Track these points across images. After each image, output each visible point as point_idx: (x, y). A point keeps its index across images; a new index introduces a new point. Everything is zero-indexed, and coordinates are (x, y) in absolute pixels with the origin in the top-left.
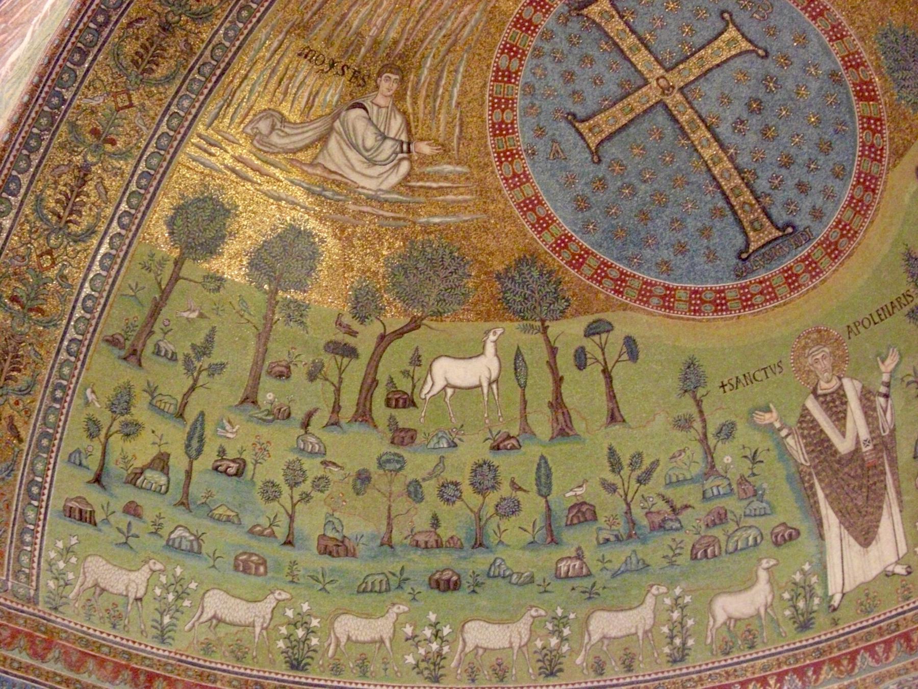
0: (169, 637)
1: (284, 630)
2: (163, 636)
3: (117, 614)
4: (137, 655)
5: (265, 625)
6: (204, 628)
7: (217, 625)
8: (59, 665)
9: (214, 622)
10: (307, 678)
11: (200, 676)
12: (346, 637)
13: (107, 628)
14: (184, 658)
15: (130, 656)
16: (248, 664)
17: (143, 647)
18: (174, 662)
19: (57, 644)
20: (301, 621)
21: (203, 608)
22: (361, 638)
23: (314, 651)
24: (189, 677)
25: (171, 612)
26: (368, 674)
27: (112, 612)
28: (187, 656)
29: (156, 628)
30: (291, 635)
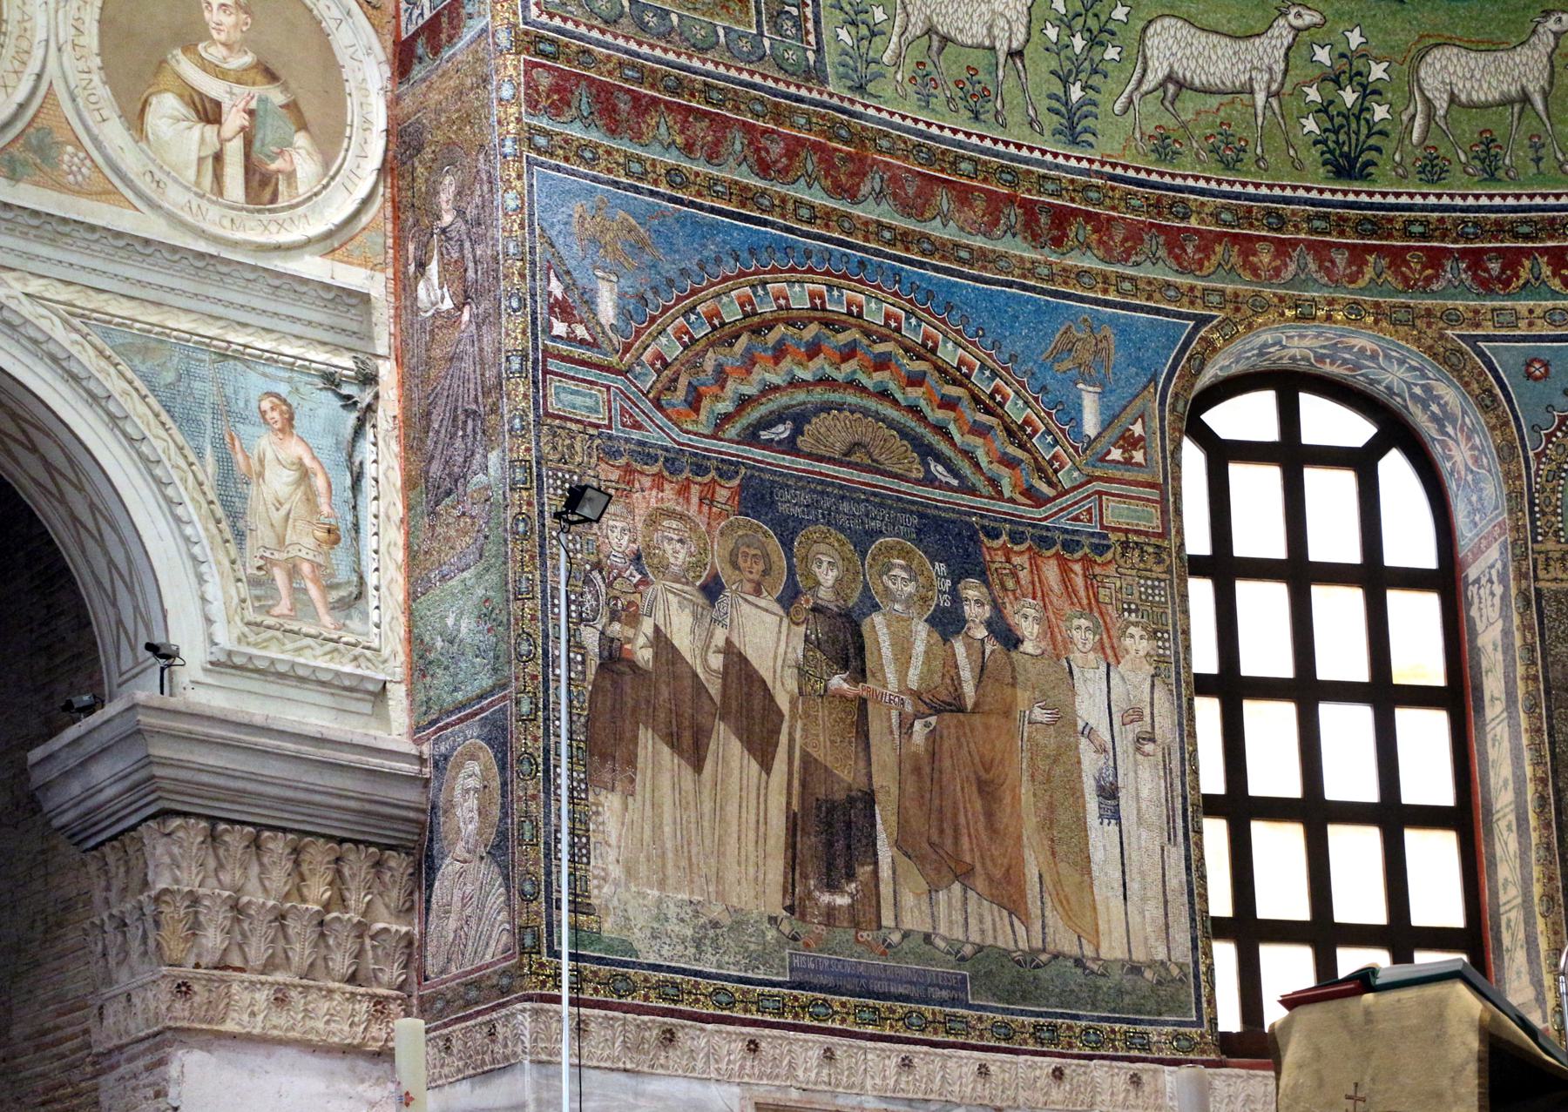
0: (1086, 130)
1: (1313, 94)
2: (1072, 127)
5: (1274, 87)
6: (1152, 104)
7: (1176, 96)
8: (885, 206)
9: (1171, 88)
10: (1371, 194)
11: (1156, 206)
12: (1445, 96)
13: (963, 121)
14: (1119, 171)
15: (1015, 178)
16: (1248, 173)
17: (1037, 154)
18: (1100, 182)
20: (1347, 71)
21: (1145, 57)
22: (1479, 96)
23: (1382, 133)
24: (1134, 210)
25: (1083, 76)
26: (1501, 174)
28: (1126, 168)
29: (1058, 113)
30: (1331, 102)
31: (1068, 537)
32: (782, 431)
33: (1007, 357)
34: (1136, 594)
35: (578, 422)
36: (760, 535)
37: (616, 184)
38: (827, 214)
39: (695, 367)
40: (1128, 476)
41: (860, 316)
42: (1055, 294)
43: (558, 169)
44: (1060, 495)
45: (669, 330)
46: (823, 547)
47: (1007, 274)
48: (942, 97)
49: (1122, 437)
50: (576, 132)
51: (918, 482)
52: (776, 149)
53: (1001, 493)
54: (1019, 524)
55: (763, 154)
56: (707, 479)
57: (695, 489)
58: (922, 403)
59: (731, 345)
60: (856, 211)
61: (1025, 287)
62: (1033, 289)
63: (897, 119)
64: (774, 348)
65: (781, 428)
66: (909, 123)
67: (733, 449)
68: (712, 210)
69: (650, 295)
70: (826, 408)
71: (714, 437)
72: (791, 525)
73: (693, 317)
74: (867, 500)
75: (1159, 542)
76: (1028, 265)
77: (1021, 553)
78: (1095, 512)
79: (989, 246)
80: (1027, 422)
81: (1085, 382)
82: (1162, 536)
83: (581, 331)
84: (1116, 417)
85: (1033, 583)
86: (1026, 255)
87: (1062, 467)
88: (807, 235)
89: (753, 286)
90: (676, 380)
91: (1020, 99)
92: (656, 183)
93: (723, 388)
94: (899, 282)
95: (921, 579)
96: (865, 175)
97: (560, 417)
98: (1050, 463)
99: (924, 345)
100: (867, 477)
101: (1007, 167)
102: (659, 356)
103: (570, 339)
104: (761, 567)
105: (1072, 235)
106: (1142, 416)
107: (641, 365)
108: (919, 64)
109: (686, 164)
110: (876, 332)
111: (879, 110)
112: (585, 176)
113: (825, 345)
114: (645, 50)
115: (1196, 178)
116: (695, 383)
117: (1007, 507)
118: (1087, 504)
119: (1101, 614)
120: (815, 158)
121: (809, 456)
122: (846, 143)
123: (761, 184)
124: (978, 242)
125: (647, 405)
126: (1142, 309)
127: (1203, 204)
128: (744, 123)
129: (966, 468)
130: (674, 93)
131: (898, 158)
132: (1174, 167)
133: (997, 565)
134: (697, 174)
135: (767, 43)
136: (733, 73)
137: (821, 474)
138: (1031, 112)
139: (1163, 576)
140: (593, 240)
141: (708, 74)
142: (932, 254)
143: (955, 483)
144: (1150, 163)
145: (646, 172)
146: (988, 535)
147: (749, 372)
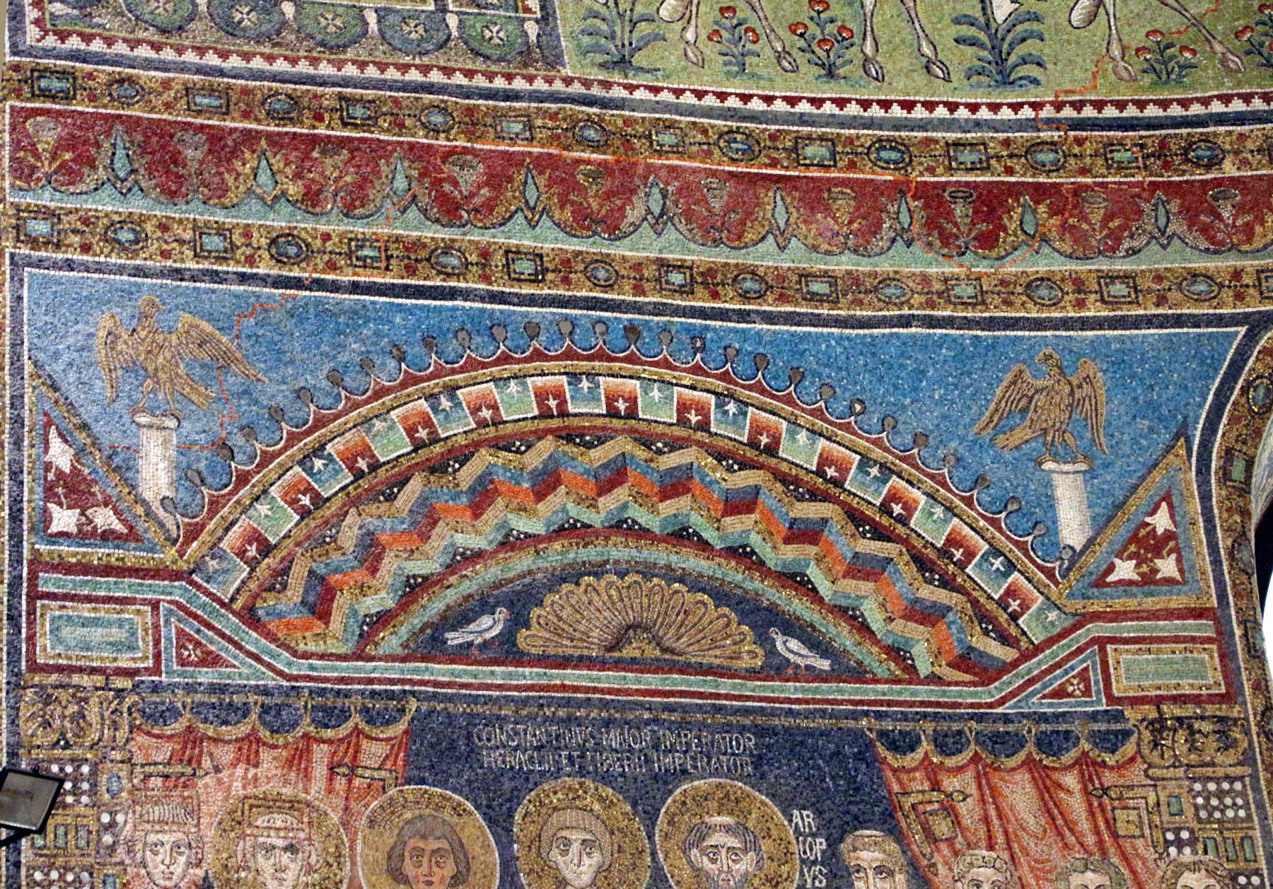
2: (1001, 60)
3: (831, 29)
4: (928, 141)
8: (671, 234)
13: (808, 82)
14: (1089, 112)
17: (941, 112)
18: (1056, 135)
19: (650, 168)
24: (1121, 167)
27: (813, 29)
28: (1099, 105)
29: (973, 42)
31: (1043, 727)
32: (489, 626)
33: (908, 439)
34: (1190, 812)
35: (94, 671)
36: (447, 814)
37: (178, 274)
38: (566, 262)
39: (321, 542)
40: (1150, 603)
41: (632, 414)
42: (991, 324)
43: (70, 265)
44: (1025, 657)
45: (274, 491)
46: (569, 816)
47: (900, 306)
48: (768, 52)
49: (1134, 538)
50: (106, 204)
51: (753, 674)
52: (469, 178)
53: (912, 669)
54: (950, 717)
55: (447, 187)
56: (343, 731)
57: (321, 754)
58: (755, 540)
59: (391, 498)
60: (621, 250)
61: (932, 322)
62: (949, 322)
63: (689, 99)
64: (472, 490)
65: (486, 621)
66: (710, 101)
67: (395, 670)
68: (355, 288)
69: (238, 440)
70: (572, 574)
71: (359, 656)
72: (507, 786)
73: (318, 464)
74: (655, 721)
75: (1224, 710)
76: (937, 286)
77: (960, 769)
78: (1095, 676)
79: (864, 266)
80: (954, 541)
81: (1056, 458)
82: (1228, 698)
83: (104, 518)
84: (1120, 506)
85: (986, 820)
86: (933, 270)
87: (1025, 607)
88: (532, 301)
89: (431, 397)
90: (285, 572)
91: (907, 34)
92: (250, 261)
93: (374, 571)
94: (703, 349)
95: (766, 845)
96: (633, 191)
97: (59, 669)
98: (1002, 604)
99: (753, 444)
100: (653, 681)
101: (889, 140)
102: (256, 537)
103: (86, 534)
104: (449, 869)
105: (1012, 227)
106: (1167, 498)
107: (222, 557)
108: (722, 10)
109: (306, 225)
110: (661, 436)
111: (656, 90)
112: (120, 270)
113: (567, 472)
114: (234, 62)
115: (1226, 99)
116: (321, 570)
117: (924, 692)
118: (1078, 664)
119: (1125, 858)
120: (542, 181)
121: (544, 661)
122: (596, 147)
123: (444, 234)
124: (844, 264)
125: (230, 623)
126: (1149, 322)
127: (1242, 137)
128: (412, 146)
129: (844, 637)
130: (285, 119)
131: (691, 158)
132: (1186, 88)
133: (913, 799)
134: (326, 237)
135: (452, 21)
136: (392, 74)
137: (564, 688)
138: (927, 50)
139: (1238, 771)
140: (132, 368)
141: (346, 82)
142: (761, 296)
143: (825, 665)
144: (1144, 90)
145: (234, 247)
146: (894, 746)
147: (425, 537)
